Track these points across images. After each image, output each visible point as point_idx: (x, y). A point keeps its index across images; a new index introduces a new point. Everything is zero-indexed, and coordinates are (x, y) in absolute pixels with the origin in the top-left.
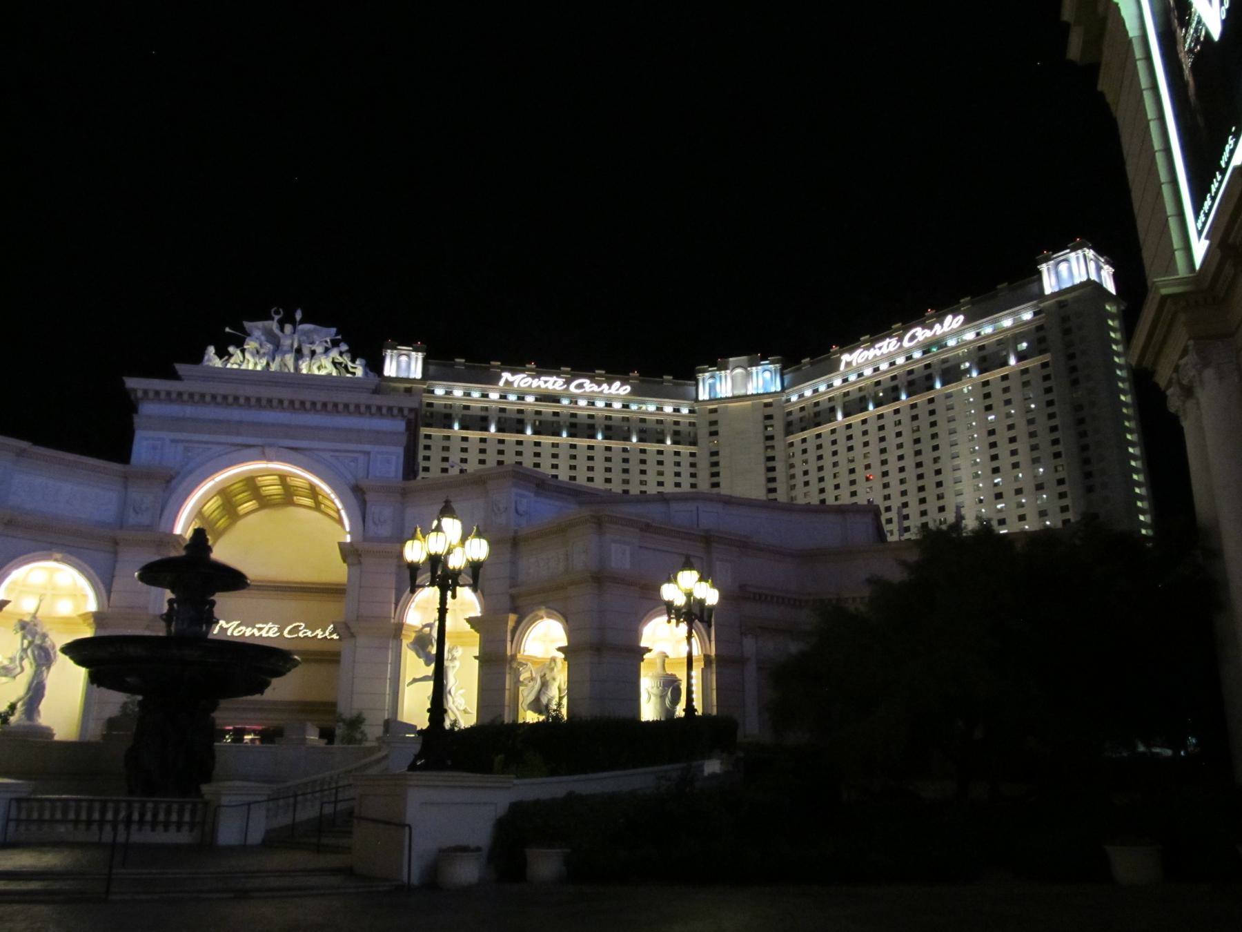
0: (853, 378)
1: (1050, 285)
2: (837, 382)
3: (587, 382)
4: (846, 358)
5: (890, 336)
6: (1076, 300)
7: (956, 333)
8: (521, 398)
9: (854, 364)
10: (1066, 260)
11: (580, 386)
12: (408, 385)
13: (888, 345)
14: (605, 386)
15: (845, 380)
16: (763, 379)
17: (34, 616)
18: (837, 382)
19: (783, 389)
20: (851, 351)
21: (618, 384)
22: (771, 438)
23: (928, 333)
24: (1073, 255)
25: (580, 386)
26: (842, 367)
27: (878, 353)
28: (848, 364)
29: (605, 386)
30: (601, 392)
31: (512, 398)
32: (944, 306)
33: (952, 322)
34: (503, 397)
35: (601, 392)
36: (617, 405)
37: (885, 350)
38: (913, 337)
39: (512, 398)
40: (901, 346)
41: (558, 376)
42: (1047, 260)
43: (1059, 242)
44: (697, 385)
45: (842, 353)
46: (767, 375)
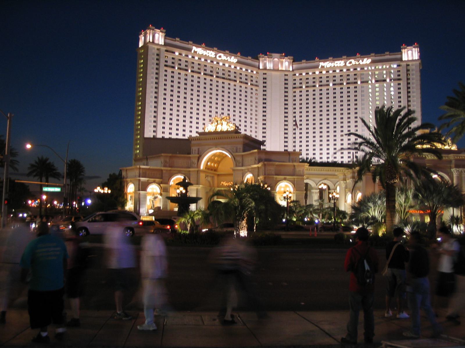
0: (324, 72)
1: (405, 58)
2: (317, 73)
3: (222, 55)
4: (322, 64)
5: (341, 60)
6: (412, 65)
7: (367, 65)
8: (200, 59)
9: (325, 67)
10: (412, 50)
11: (220, 57)
12: (159, 47)
13: (340, 63)
14: (229, 58)
15: (321, 72)
16: (286, 64)
17: (448, 211)
18: (317, 73)
19: (293, 70)
20: (324, 62)
21: (233, 57)
22: (264, 83)
23: (357, 63)
24: (414, 49)
25: (220, 57)
26: (320, 67)
27: (336, 66)
28: (323, 67)
29: (229, 58)
30: (227, 60)
31: (196, 58)
32: (365, 53)
33: (367, 61)
34: (193, 57)
35: (227, 60)
36: (233, 67)
37: (339, 65)
38: (350, 63)
39: (196, 58)
40: (345, 65)
41: (213, 51)
42: (405, 48)
43: (409, 44)
44: (259, 63)
45: (320, 62)
46: (287, 63)
